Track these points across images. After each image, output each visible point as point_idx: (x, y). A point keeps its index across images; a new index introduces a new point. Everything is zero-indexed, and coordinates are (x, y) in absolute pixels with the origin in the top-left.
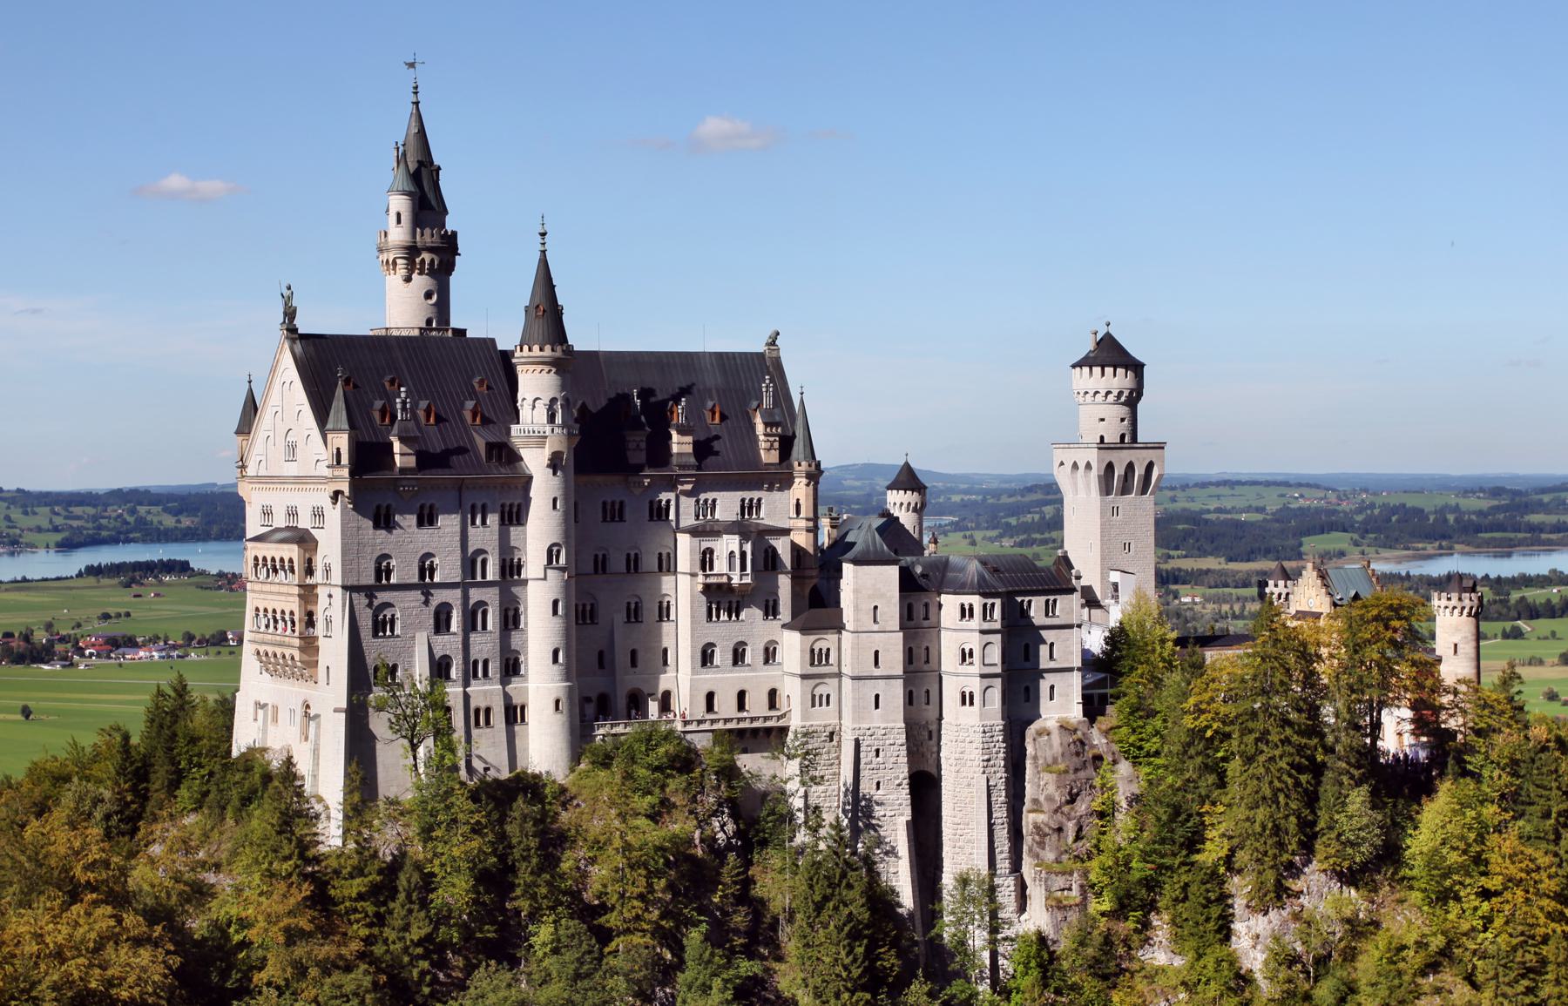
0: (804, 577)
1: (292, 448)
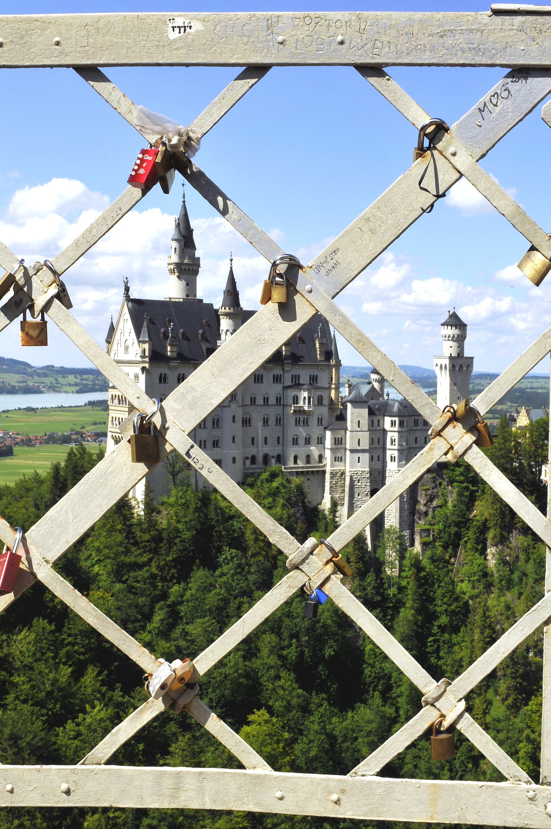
0: (333, 408)
1: (127, 348)
